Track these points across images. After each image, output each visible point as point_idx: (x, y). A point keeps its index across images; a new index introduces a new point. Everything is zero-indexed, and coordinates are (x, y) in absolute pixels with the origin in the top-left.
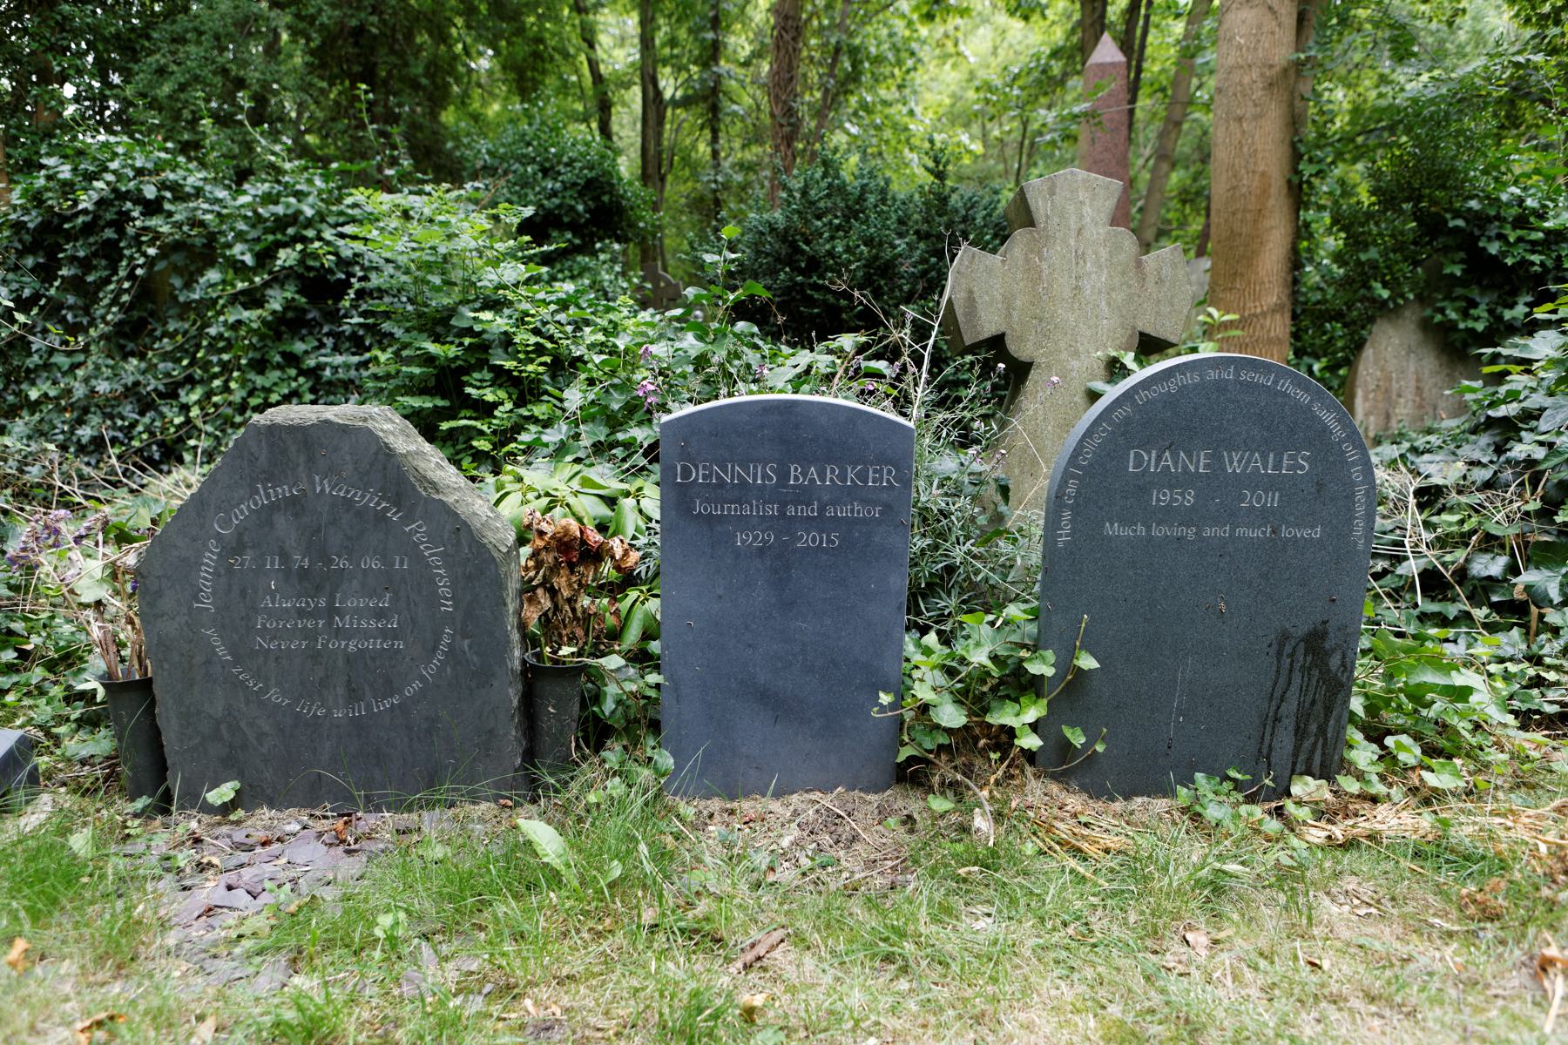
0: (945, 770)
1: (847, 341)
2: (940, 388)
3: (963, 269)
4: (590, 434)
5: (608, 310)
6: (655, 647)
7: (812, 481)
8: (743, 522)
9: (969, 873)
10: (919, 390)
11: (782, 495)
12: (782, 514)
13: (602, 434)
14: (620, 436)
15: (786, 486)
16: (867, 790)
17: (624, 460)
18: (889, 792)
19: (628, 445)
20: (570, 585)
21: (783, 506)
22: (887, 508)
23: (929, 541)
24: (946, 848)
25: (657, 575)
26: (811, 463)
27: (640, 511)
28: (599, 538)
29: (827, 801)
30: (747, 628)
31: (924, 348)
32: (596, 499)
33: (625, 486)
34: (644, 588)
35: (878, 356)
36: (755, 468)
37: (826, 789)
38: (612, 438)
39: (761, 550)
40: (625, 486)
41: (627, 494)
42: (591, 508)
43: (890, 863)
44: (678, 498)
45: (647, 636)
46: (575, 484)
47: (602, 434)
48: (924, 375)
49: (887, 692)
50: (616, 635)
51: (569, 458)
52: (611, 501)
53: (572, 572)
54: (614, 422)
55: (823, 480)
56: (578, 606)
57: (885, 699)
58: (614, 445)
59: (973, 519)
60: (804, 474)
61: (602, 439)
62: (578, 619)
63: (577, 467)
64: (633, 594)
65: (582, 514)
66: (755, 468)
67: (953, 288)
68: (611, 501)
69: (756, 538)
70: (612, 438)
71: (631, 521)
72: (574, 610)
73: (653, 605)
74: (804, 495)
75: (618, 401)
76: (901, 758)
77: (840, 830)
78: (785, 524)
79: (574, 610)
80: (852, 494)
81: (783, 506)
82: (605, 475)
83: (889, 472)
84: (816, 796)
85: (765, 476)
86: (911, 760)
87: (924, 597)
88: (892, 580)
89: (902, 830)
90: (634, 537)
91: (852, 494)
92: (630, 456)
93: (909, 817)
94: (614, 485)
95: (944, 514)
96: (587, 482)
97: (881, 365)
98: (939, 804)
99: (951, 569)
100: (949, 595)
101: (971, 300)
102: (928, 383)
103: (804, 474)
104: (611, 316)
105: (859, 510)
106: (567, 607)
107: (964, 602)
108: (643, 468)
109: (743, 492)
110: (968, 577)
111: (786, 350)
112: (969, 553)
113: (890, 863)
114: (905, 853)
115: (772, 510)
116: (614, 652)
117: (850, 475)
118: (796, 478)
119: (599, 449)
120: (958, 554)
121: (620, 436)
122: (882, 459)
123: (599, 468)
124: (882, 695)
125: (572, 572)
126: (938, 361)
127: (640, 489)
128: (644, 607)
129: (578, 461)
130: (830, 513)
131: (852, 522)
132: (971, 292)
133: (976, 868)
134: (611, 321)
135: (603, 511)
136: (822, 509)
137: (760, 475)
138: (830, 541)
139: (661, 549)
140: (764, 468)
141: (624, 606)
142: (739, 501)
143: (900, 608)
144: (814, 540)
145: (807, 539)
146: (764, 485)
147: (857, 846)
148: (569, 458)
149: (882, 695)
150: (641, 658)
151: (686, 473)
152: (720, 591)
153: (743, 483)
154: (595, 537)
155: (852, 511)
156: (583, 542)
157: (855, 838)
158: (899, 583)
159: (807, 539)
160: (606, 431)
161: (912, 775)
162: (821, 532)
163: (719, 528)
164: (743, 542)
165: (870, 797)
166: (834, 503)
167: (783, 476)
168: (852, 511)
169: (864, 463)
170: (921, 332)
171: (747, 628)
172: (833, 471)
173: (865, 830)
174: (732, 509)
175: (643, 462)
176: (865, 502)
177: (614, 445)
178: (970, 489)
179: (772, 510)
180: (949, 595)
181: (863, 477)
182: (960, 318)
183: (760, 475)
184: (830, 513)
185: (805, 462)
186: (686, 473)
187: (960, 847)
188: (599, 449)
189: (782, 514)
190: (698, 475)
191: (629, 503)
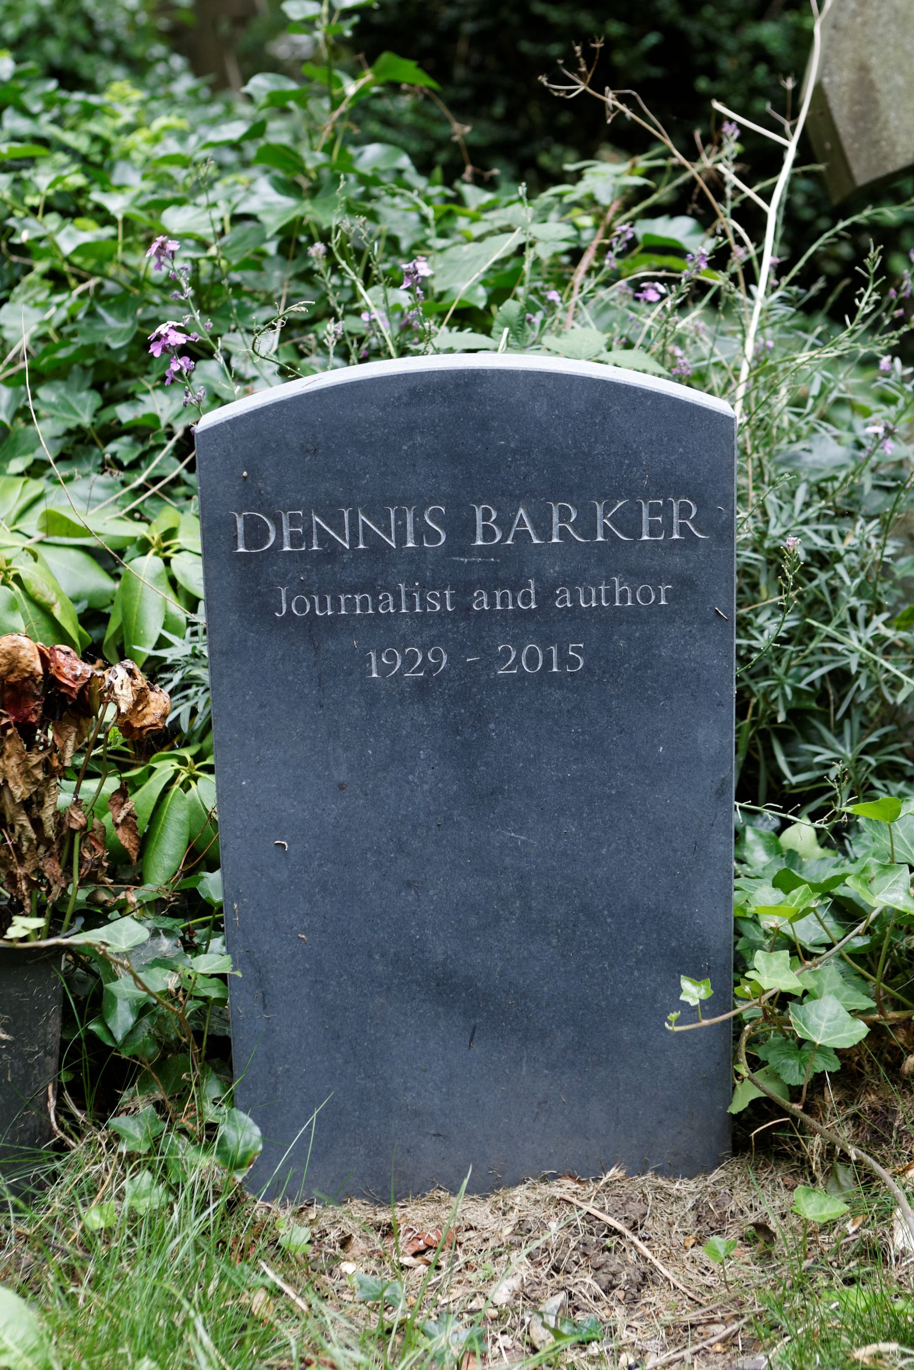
0: (833, 1129)
1: (607, 176)
2: (804, 280)
3: (845, 20)
4: (67, 407)
5: (89, 112)
6: (212, 885)
7: (523, 536)
8: (381, 629)
9: (879, 1356)
10: (759, 291)
11: (461, 570)
12: (463, 609)
13: (84, 409)
14: (125, 413)
15: (467, 550)
16: (670, 1172)
17: (134, 466)
18: (717, 1174)
19: (141, 432)
20: (27, 773)
21: (464, 590)
22: (684, 586)
23: (791, 621)
24: (836, 1302)
25: (208, 727)
26: (516, 499)
27: (173, 582)
28: (84, 669)
29: (589, 1200)
30: (401, 848)
31: (767, 196)
32: (73, 553)
33: (138, 530)
34: (187, 753)
35: (673, 210)
36: (400, 515)
37: (584, 1173)
38: (106, 415)
39: (422, 688)
40: (138, 530)
41: (144, 546)
42: (66, 577)
43: (720, 1331)
44: (242, 583)
45: (200, 857)
46: (32, 523)
47: (84, 409)
48: (768, 259)
49: (697, 976)
50: (126, 866)
51: (18, 465)
52: (109, 558)
53: (31, 745)
54: (112, 378)
55: (545, 534)
56: (47, 814)
57: (693, 992)
58: (112, 431)
59: (885, 569)
60: (505, 524)
61: (86, 420)
62: (48, 843)
63: (36, 486)
64: (165, 768)
65: (49, 597)
66: (400, 515)
67: (825, 61)
68: (109, 558)
69: (409, 660)
70: (106, 415)
71: (154, 609)
72: (37, 824)
73: (205, 791)
74: (505, 569)
75: (116, 334)
76: (739, 1105)
77: (615, 1261)
78: (469, 630)
79: (37, 824)
80: (605, 560)
81: (464, 590)
82: (93, 504)
83: (685, 511)
84: (565, 1188)
85: (422, 532)
86: (762, 1108)
87: (785, 737)
88: (701, 734)
89: (746, 1254)
90: (163, 642)
91: (605, 560)
92: (147, 455)
93: (762, 1228)
94: (109, 525)
95: (823, 559)
96: (55, 524)
97: (678, 229)
98: (817, 1205)
99: (841, 678)
100: (839, 734)
101: (865, 88)
102: (780, 270)
103: (505, 524)
104: (94, 127)
105: (624, 593)
106: (24, 820)
107: (869, 750)
108: (177, 481)
109: (376, 567)
110: (877, 695)
111: (475, 196)
112: (879, 639)
113: (720, 1331)
114: (754, 1305)
115: (443, 601)
116: (123, 909)
117: (602, 520)
118: (488, 533)
119: (78, 445)
120: (854, 646)
121: (125, 413)
122: (667, 485)
123: (80, 488)
124: (686, 984)
125: (31, 745)
126: (797, 233)
127: (170, 534)
128: (186, 795)
129: (36, 469)
130: (563, 601)
131: (610, 619)
132: (863, 68)
133: (894, 1346)
134: (95, 138)
135: (95, 580)
136: (546, 595)
137: (412, 530)
138: (565, 660)
139: (211, 667)
140: (419, 515)
141: (142, 800)
142: (369, 586)
143: (721, 792)
144: (532, 659)
145: (517, 659)
146: (420, 551)
147: (652, 1296)
148: (18, 465)
149: (686, 984)
150: (187, 910)
151: (256, 533)
152: (341, 775)
153: (377, 548)
154: (73, 667)
155: (610, 597)
156: (51, 680)
157: (646, 1279)
158: (719, 741)
159: (517, 659)
160: (92, 400)
161: (763, 1139)
162: (545, 642)
163: (331, 645)
164: (384, 670)
165: (679, 1186)
166: (571, 581)
167: (461, 529)
168: (610, 597)
169: (630, 494)
170: (760, 161)
171: (401, 848)
172: (564, 515)
173: (667, 1258)
174: (357, 604)
175: (178, 469)
176: (634, 575)
177: (111, 432)
178: (877, 501)
179: (443, 601)
180: (839, 734)
181: (629, 522)
182: (844, 127)
183: (412, 530)
184: (563, 601)
185: (507, 499)
186: (256, 533)
187: (858, 1298)
188: (78, 445)
189: (463, 609)
190: (281, 537)
191: (145, 566)
